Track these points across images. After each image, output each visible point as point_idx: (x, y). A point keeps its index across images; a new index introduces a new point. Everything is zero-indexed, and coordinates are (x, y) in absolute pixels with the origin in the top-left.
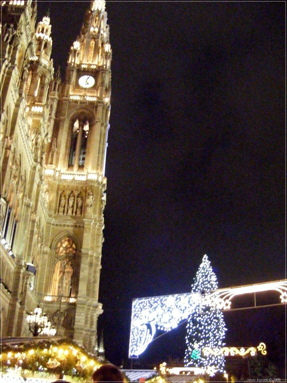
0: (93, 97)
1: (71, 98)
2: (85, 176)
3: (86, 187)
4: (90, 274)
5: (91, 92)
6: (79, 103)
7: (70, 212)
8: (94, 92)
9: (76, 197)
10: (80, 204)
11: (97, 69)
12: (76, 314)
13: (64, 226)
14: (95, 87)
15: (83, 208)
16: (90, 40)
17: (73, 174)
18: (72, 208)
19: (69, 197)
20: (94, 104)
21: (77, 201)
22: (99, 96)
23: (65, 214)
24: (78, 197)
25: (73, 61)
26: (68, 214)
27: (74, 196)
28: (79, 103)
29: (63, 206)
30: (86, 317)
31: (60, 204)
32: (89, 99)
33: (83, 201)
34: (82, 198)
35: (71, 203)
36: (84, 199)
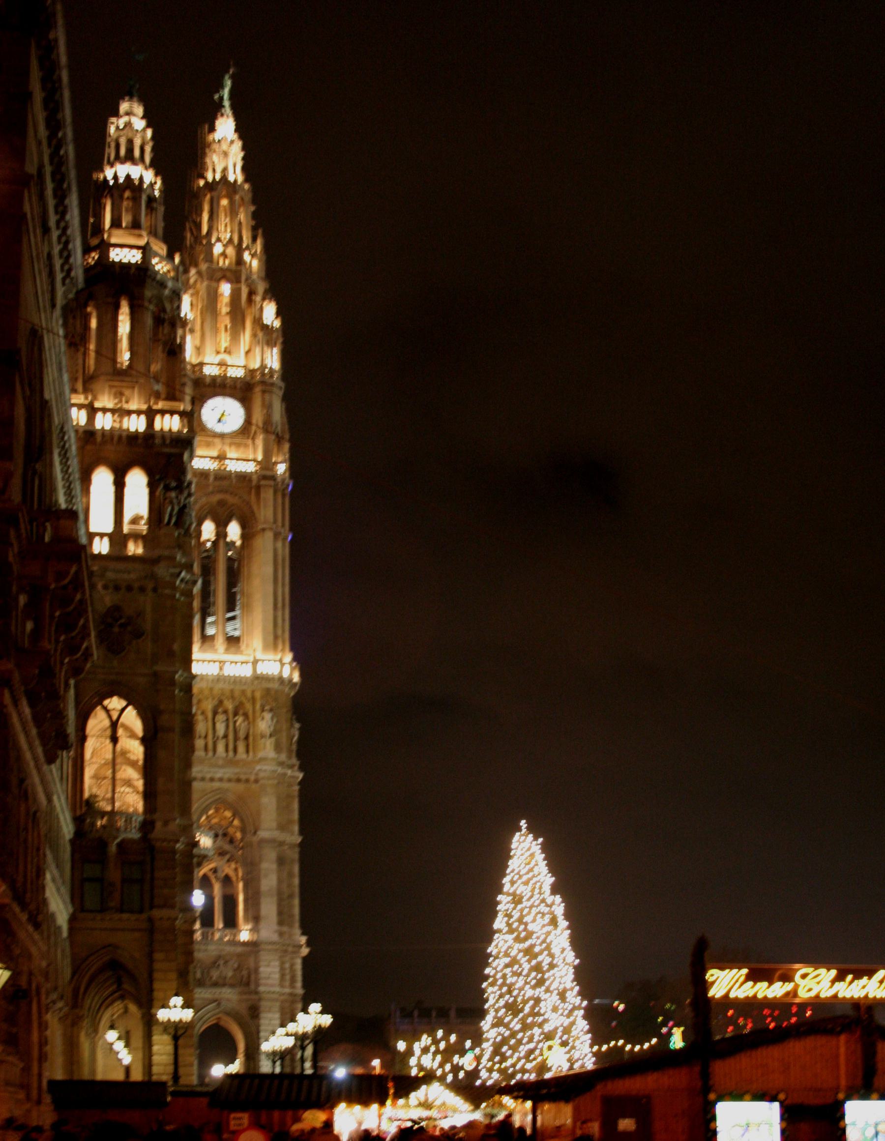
3: (253, 692)
4: (280, 881)
5: (238, 445)
6: (211, 478)
7: (221, 748)
8: (246, 446)
9: (231, 716)
10: (242, 734)
11: (248, 378)
12: (262, 963)
13: (212, 780)
14: (245, 430)
15: (251, 739)
16: (214, 284)
18: (224, 740)
19: (215, 713)
20: (250, 480)
21: (235, 722)
22: (260, 457)
23: (210, 754)
24: (236, 714)
26: (217, 755)
27: (225, 712)
28: (211, 478)
29: (203, 735)
30: (282, 969)
32: (233, 466)
33: (249, 723)
34: (246, 715)
35: (221, 728)
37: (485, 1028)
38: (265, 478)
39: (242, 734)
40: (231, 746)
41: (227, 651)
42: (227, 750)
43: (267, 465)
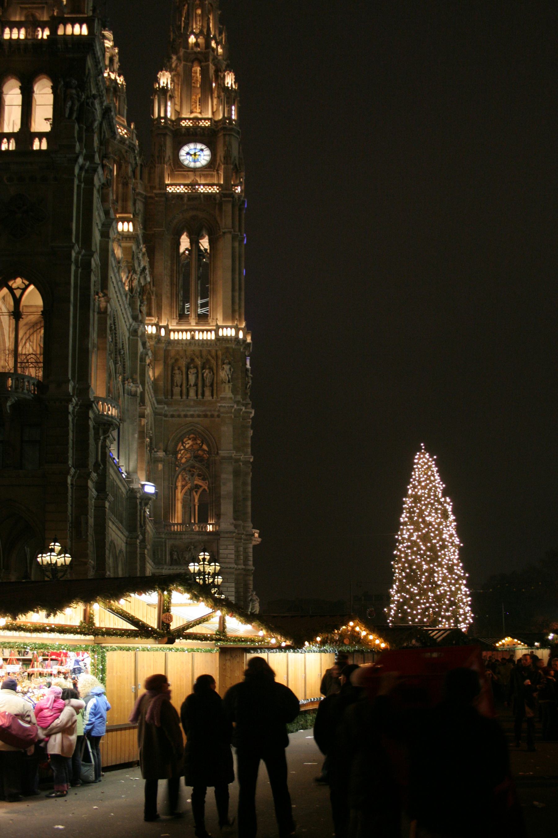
0: (212, 185)
1: (170, 190)
2: (213, 332)
3: (216, 351)
4: (235, 487)
5: (206, 176)
6: (186, 199)
7: (192, 393)
8: (212, 176)
9: (200, 370)
10: (208, 382)
11: (213, 127)
12: (221, 547)
13: (186, 416)
14: (211, 165)
15: (215, 385)
16: (189, 64)
17: (191, 331)
18: (195, 387)
19: (188, 368)
20: (215, 199)
21: (203, 374)
23: (184, 397)
24: (203, 368)
25: (162, 115)
26: (189, 398)
27: (196, 367)
28: (186, 199)
29: (179, 384)
30: (237, 551)
31: (172, 381)
32: (202, 189)
33: (213, 374)
34: (211, 369)
35: (192, 379)
36: (215, 372)
37: (392, 592)
38: (225, 195)
39: (208, 382)
40: (200, 391)
41: (197, 324)
42: (197, 395)
43: (226, 188)
